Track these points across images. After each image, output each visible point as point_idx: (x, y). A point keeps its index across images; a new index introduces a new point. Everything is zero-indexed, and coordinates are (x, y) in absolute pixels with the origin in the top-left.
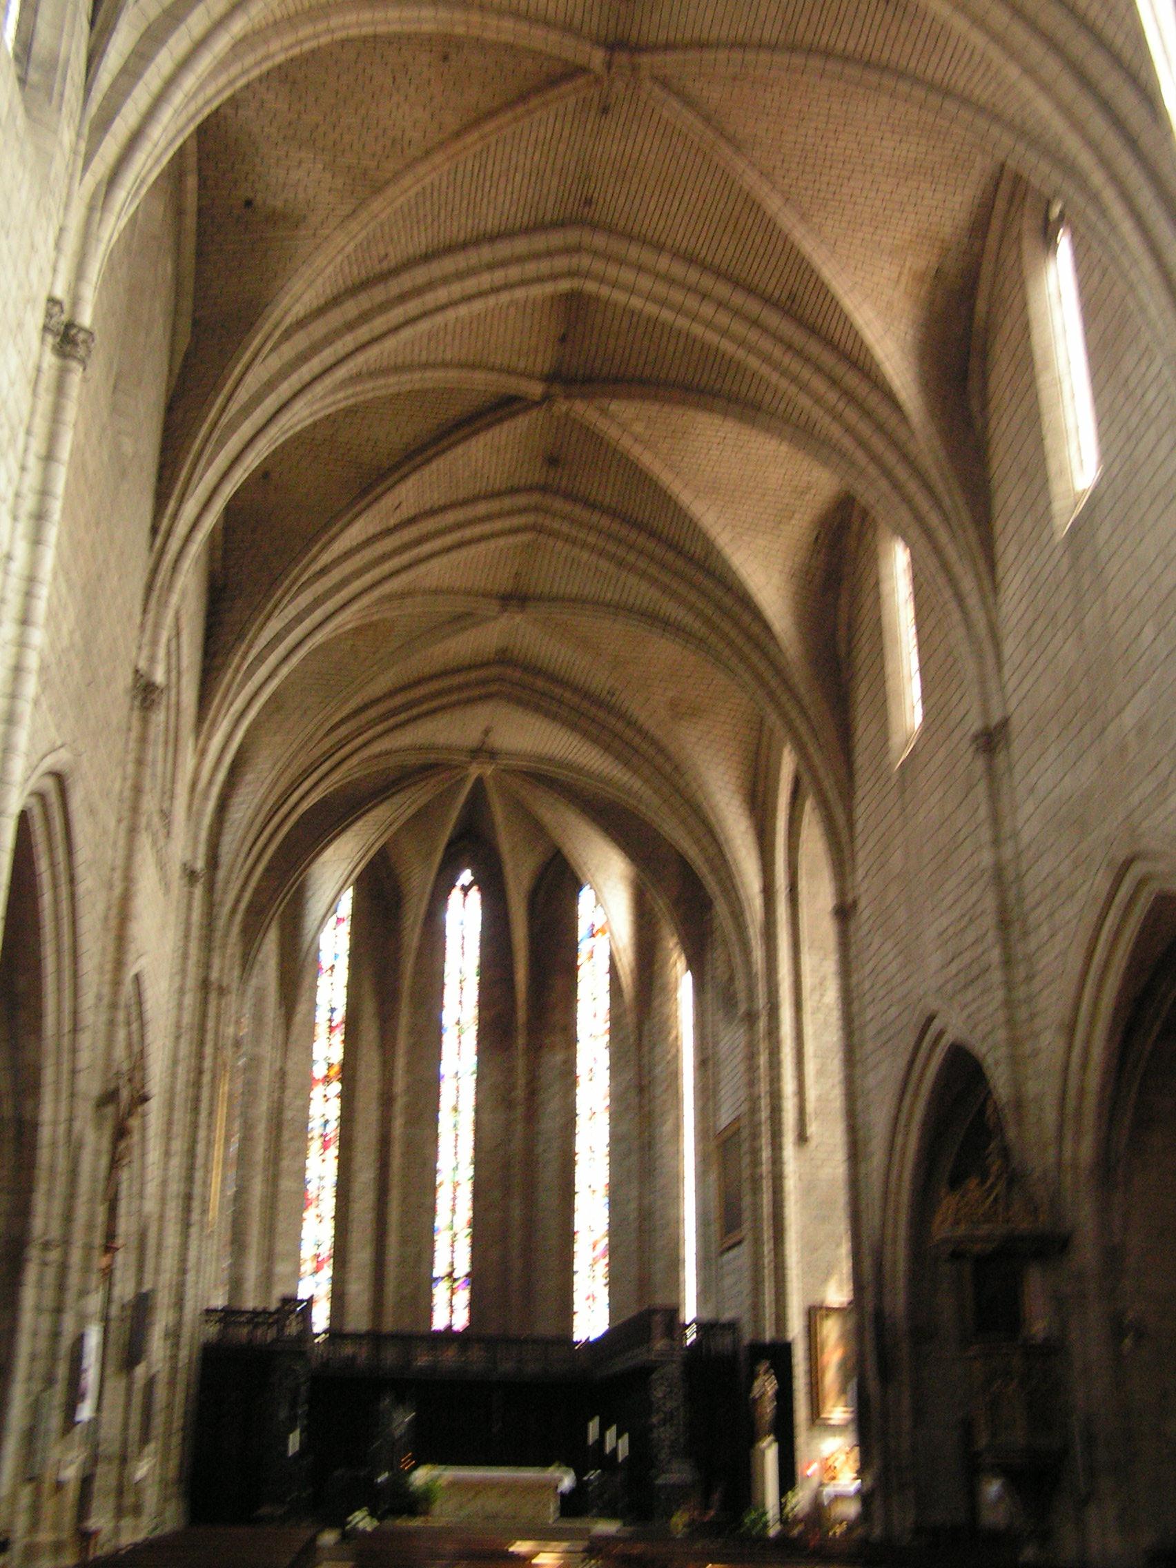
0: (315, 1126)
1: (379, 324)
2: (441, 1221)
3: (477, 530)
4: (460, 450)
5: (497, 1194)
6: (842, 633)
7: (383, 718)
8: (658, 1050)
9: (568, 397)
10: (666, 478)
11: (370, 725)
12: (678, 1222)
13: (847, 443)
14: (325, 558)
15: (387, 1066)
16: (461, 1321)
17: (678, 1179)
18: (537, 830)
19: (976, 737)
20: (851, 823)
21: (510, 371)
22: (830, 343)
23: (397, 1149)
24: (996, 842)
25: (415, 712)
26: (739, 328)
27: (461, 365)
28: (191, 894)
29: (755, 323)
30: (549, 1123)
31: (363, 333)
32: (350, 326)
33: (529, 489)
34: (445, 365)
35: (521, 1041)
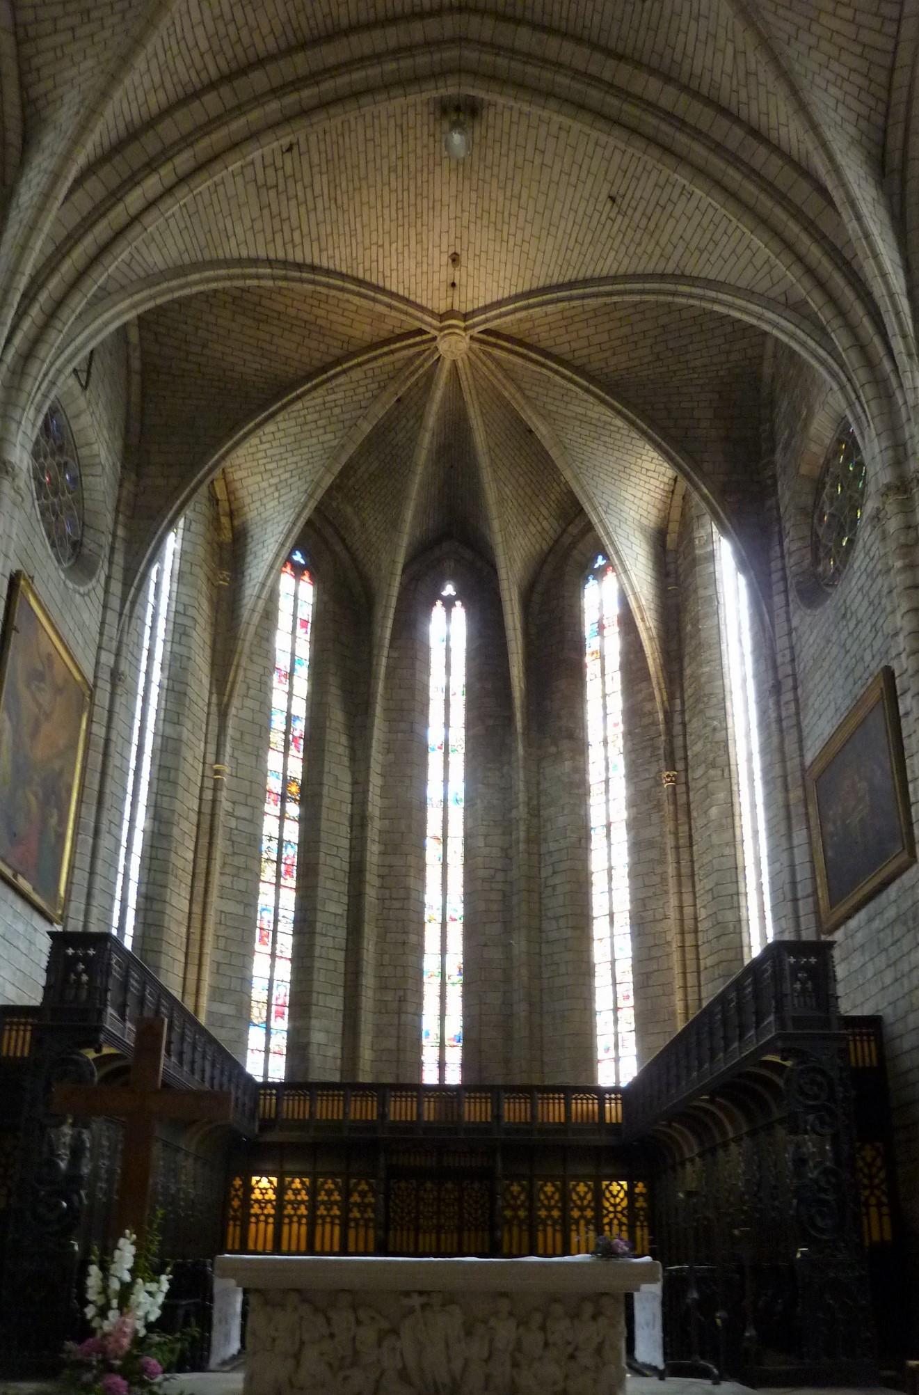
0: (269, 848)
2: (430, 963)
5: (495, 929)
23: (372, 878)
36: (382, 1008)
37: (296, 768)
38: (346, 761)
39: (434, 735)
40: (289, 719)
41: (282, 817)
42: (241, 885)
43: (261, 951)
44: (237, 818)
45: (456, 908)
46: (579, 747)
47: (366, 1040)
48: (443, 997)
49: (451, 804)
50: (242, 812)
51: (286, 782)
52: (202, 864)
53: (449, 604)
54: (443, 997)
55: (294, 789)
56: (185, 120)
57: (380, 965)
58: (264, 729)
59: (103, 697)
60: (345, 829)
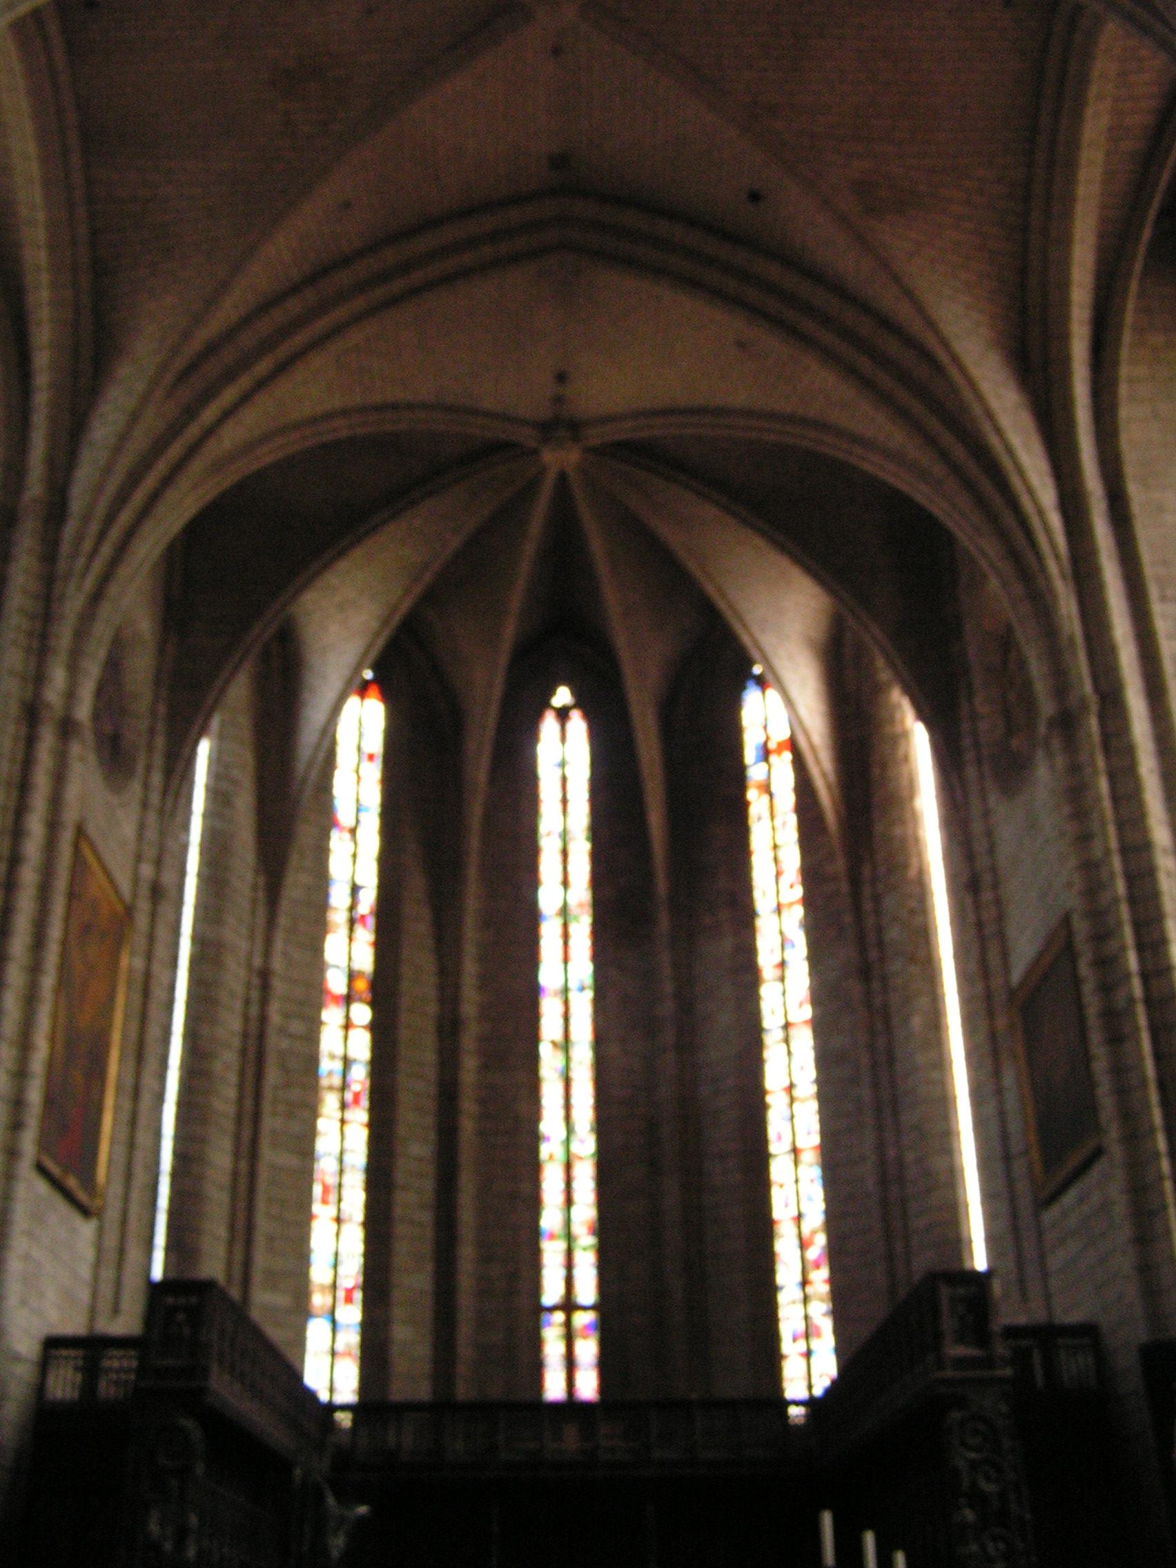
8: (889, 902)
12: (952, 1177)
16: (588, 1386)
17: (945, 1103)
23: (468, 1106)
35: (664, 922)
37: (365, 960)
38: (430, 942)
39: (548, 897)
40: (355, 889)
41: (348, 1026)
42: (295, 1127)
43: (322, 1213)
44: (291, 1036)
45: (586, 1145)
46: (745, 916)
47: (465, 1330)
48: (569, 1265)
49: (572, 996)
50: (297, 1027)
51: (352, 976)
52: (249, 1103)
53: (563, 714)
54: (569, 1265)
55: (361, 985)
56: (265, 326)
58: (320, 905)
59: (142, 920)
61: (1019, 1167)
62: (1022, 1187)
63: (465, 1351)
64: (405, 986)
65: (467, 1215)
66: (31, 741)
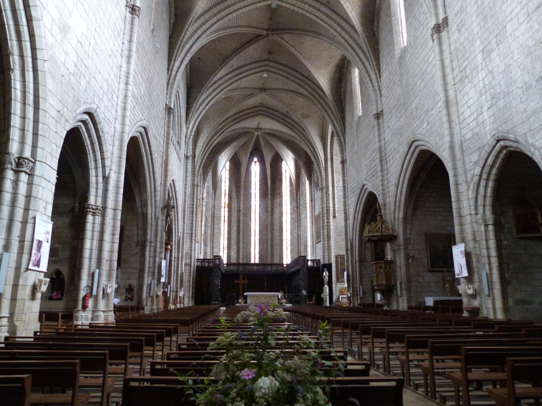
1: (223, 14)
3: (253, 71)
4: (247, 50)
5: (265, 232)
6: (342, 94)
7: (233, 120)
8: (301, 198)
9: (273, 35)
10: (298, 55)
11: (230, 122)
13: (343, 41)
14: (215, 79)
15: (239, 204)
17: (306, 227)
18: (272, 147)
19: (375, 115)
20: (345, 141)
21: (258, 28)
22: (338, 14)
23: (241, 222)
24: (380, 141)
25: (241, 119)
26: (315, 11)
27: (245, 27)
28: (187, 162)
29: (319, 10)
30: (276, 216)
31: (219, 17)
32: (215, 15)
33: (264, 60)
34: (241, 27)
35: (270, 197)
36: (243, 248)
37: (227, 202)
43: (222, 237)
53: (255, 162)
57: (243, 239)
60: (236, 213)
61: (314, 238)
62: (314, 241)
63: (241, 256)
64: (233, 205)
65: (241, 238)
66: (194, 189)
